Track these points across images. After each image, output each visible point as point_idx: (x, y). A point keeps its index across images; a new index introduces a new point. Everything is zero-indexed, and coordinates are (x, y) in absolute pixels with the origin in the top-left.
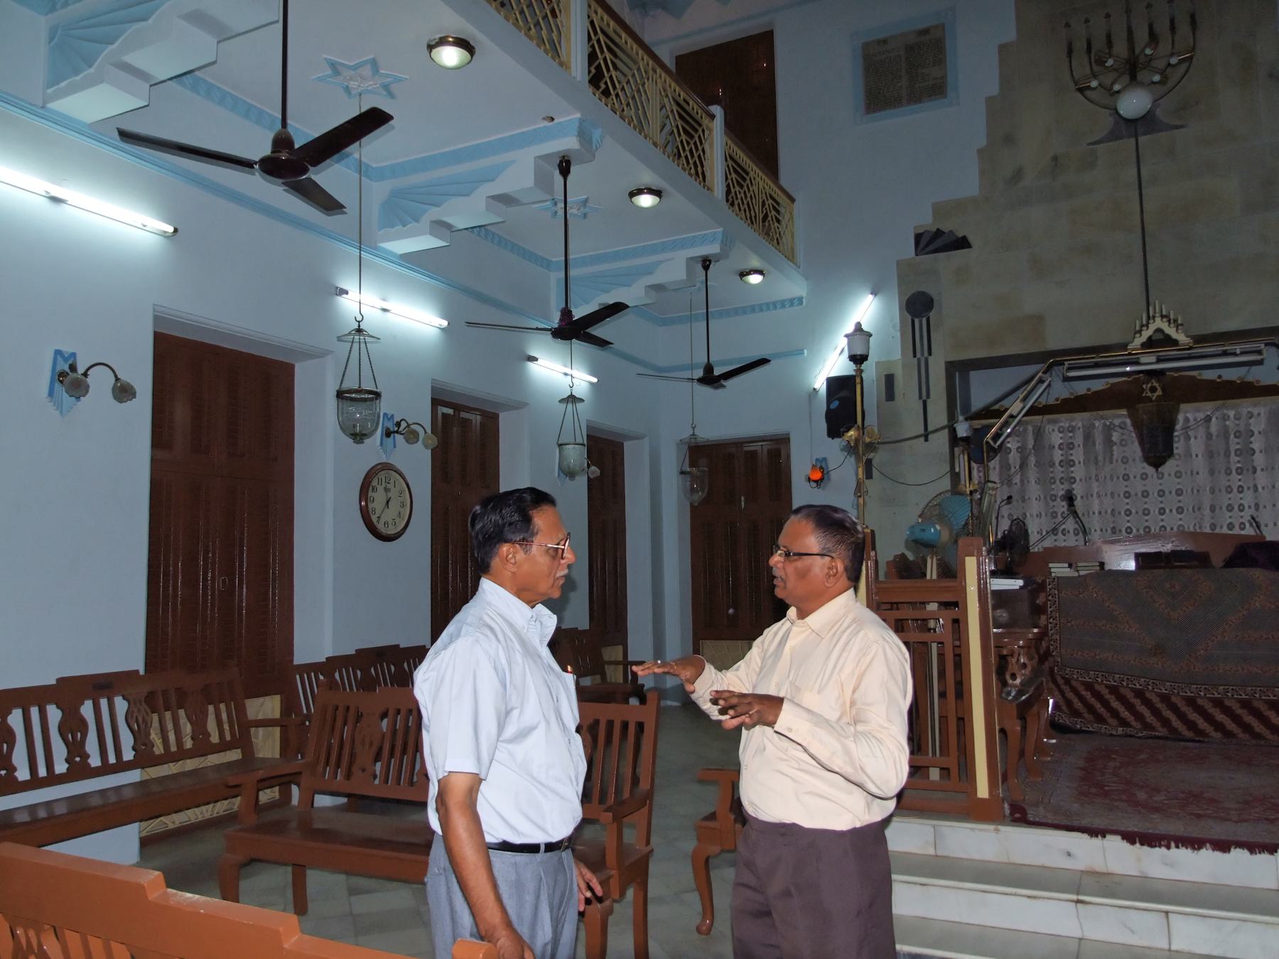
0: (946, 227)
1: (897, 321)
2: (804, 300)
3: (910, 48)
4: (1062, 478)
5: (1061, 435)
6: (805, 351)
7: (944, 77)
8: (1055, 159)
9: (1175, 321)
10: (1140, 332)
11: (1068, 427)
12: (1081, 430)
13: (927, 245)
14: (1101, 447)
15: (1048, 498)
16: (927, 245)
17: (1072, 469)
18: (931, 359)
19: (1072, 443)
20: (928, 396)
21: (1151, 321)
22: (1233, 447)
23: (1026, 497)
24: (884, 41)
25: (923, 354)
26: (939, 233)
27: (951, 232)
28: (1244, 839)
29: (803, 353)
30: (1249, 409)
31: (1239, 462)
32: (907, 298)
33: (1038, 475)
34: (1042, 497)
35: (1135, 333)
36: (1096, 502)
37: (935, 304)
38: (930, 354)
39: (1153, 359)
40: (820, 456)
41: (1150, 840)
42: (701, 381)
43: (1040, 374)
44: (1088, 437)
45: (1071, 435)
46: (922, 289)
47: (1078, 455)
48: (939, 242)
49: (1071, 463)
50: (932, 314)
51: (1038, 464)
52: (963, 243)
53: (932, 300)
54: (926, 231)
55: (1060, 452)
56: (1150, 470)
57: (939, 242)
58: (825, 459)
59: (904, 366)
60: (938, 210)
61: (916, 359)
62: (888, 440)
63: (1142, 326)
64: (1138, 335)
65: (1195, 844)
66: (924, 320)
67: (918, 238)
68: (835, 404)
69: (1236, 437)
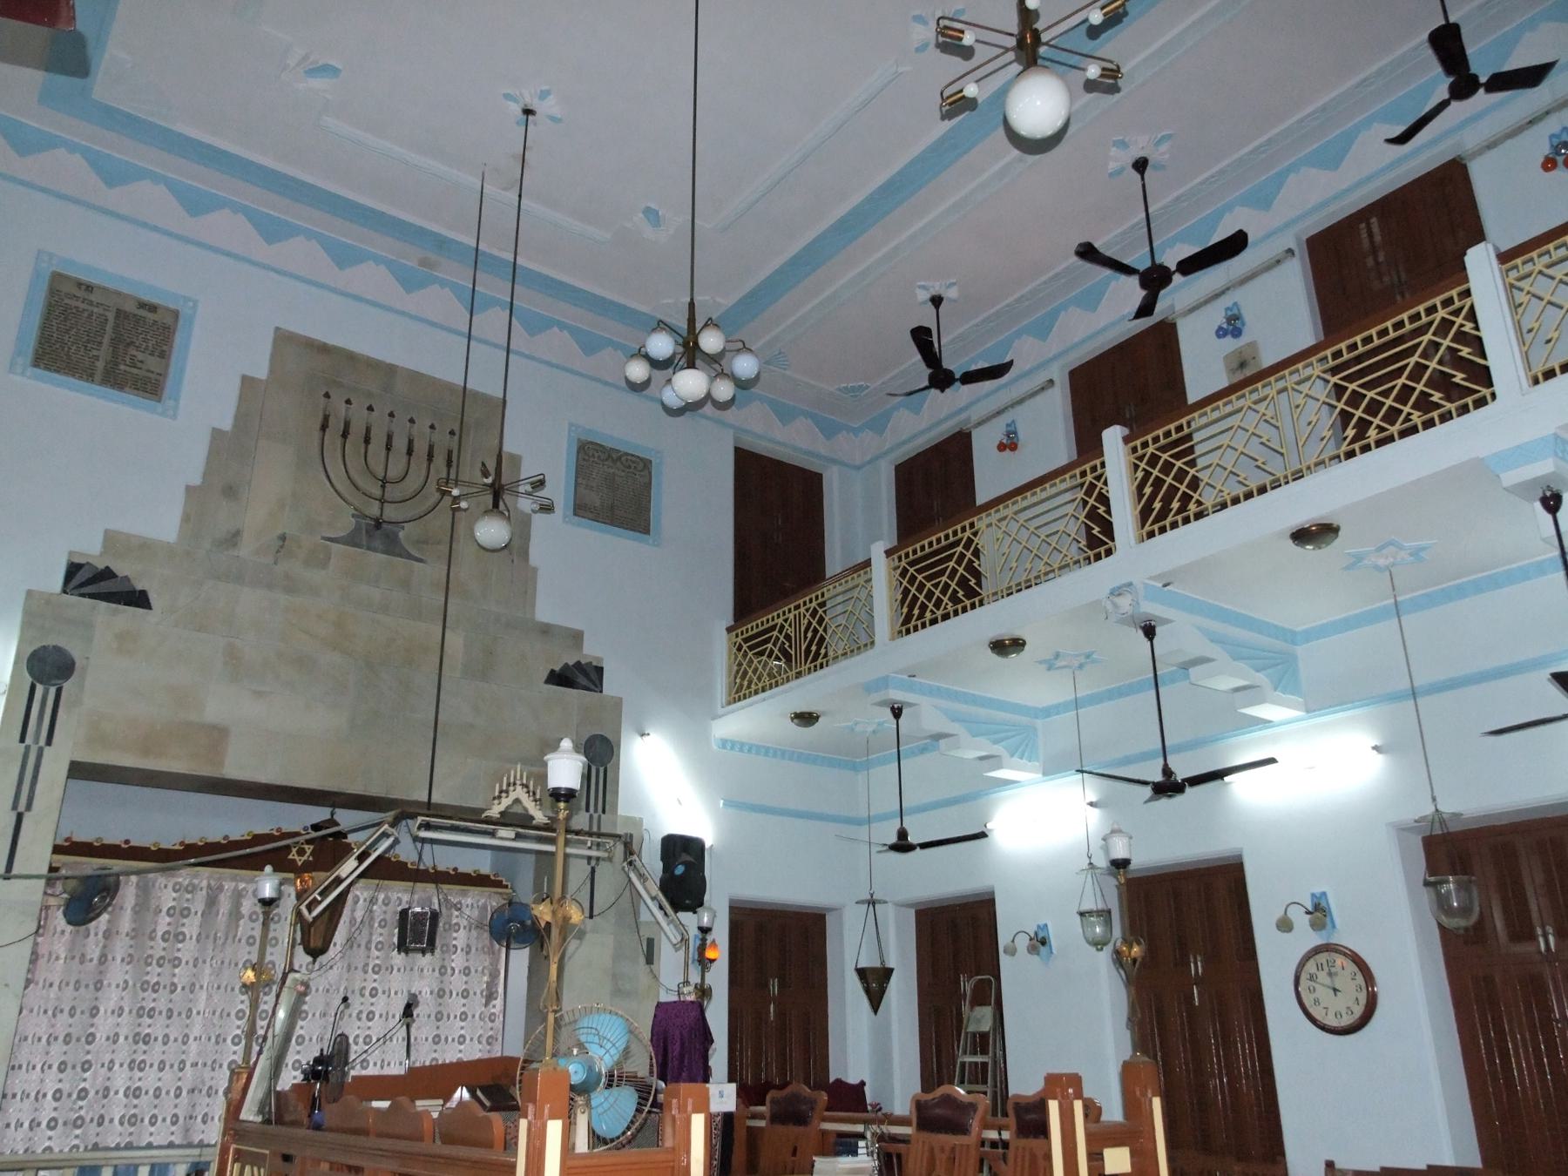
0: (121, 568)
3: (119, 313)
4: (162, 958)
5: (174, 895)
7: (163, 375)
8: (283, 538)
9: (534, 794)
10: (499, 797)
11: (188, 886)
12: (204, 892)
13: (82, 585)
14: (225, 919)
15: (139, 985)
16: (82, 585)
17: (180, 946)
18: (47, 750)
19: (188, 909)
20: (29, 807)
21: (511, 788)
22: (376, 938)
23: (105, 982)
24: (89, 288)
25: (36, 741)
26: (107, 574)
27: (126, 578)
30: (400, 895)
31: (378, 958)
33: (131, 951)
34: (131, 983)
35: (494, 798)
36: (203, 996)
38: (49, 742)
39: (512, 835)
43: (386, 826)
44: (212, 902)
45: (189, 896)
46: (61, 642)
47: (191, 927)
48: (104, 586)
49: (180, 937)
50: (68, 686)
51: (135, 934)
52: (139, 599)
53: (73, 664)
54: (88, 563)
55: (168, 919)
56: (310, 959)
57: (104, 586)
60: (112, 540)
61: (24, 745)
63: (501, 792)
64: (496, 802)
66: (53, 690)
67: (73, 570)
69: (380, 926)
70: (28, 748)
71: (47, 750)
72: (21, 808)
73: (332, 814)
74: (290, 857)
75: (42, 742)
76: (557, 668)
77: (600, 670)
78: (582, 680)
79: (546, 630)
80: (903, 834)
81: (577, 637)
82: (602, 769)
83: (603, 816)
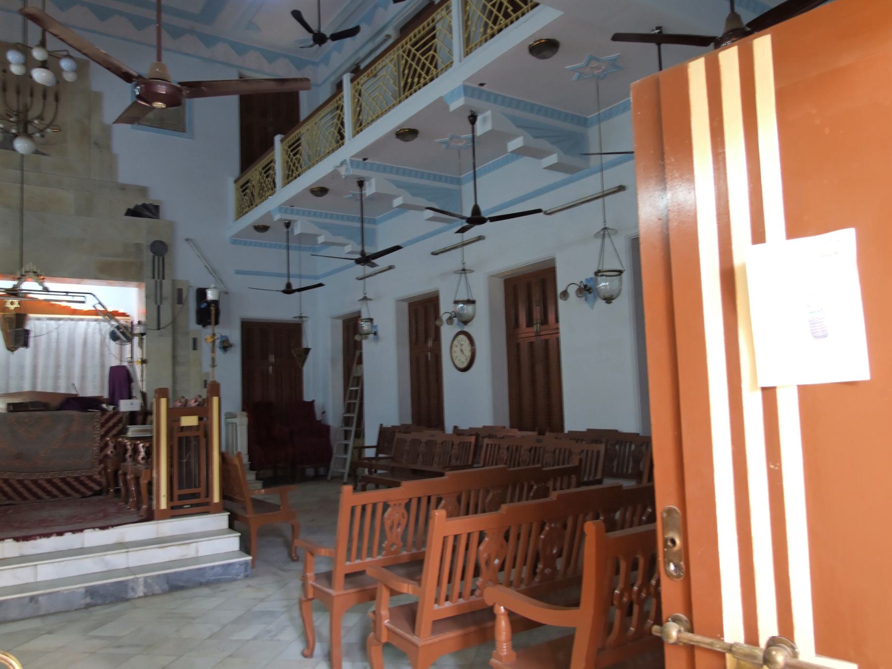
28: (71, 529)
41: (26, 538)
65: (48, 535)
76: (132, 207)
77: (157, 208)
78: (147, 213)
79: (123, 188)
80: (289, 285)
81: (143, 191)
82: (161, 258)
83: (163, 281)
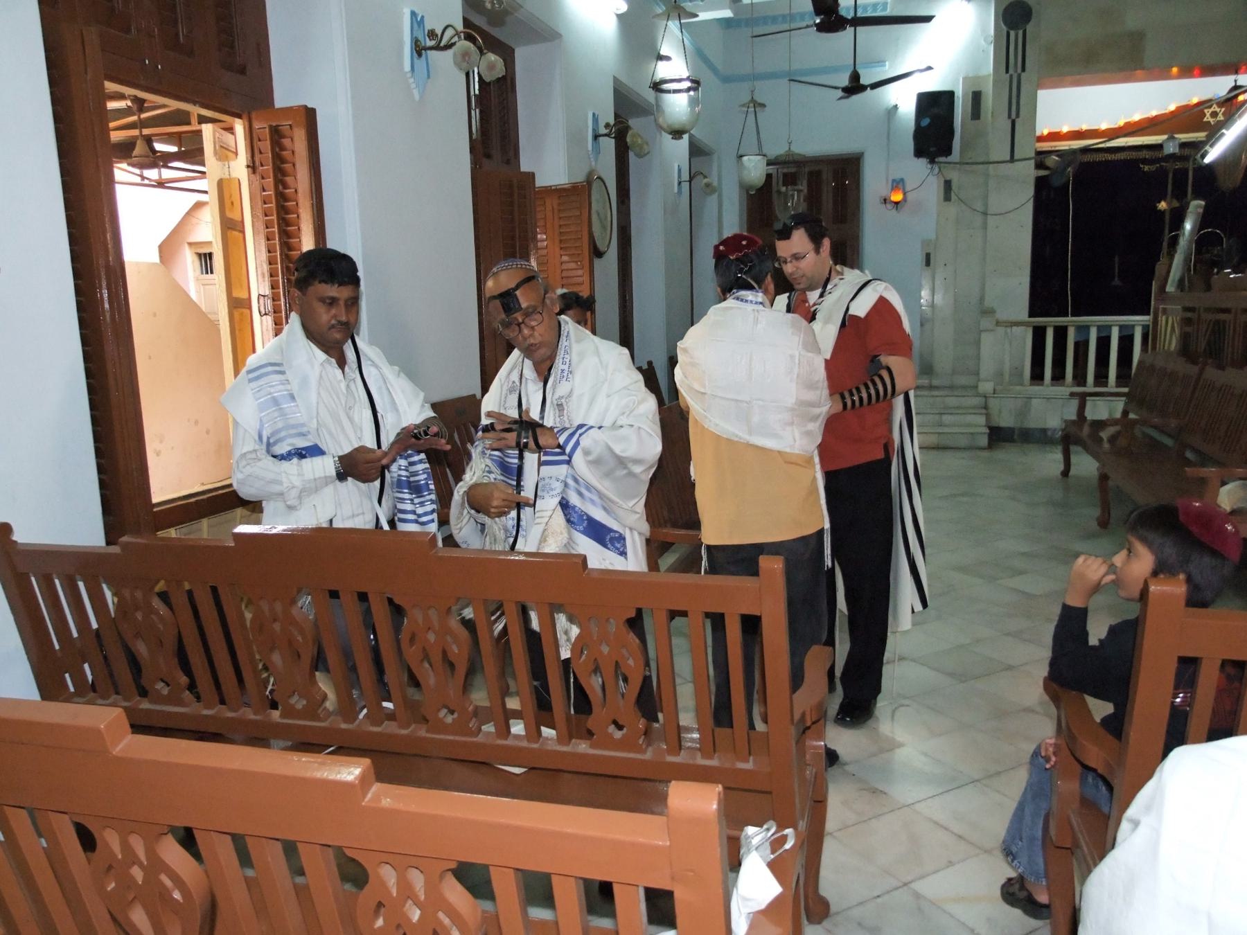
1: (991, 31)
2: (889, 6)
6: (887, 63)
20: (1018, 115)
25: (1016, 71)
29: (885, 66)
32: (1004, 7)
37: (1034, 15)
38: (1023, 70)
40: (898, 176)
42: (845, 90)
50: (1030, 28)
58: (902, 180)
59: (995, 82)
61: (1008, 75)
62: (970, 161)
66: (1021, 32)
68: (926, 122)
70: (1011, 76)
71: (1023, 74)
72: (1014, 116)
73: (1236, 81)
74: (1205, 119)
75: (1019, 70)
